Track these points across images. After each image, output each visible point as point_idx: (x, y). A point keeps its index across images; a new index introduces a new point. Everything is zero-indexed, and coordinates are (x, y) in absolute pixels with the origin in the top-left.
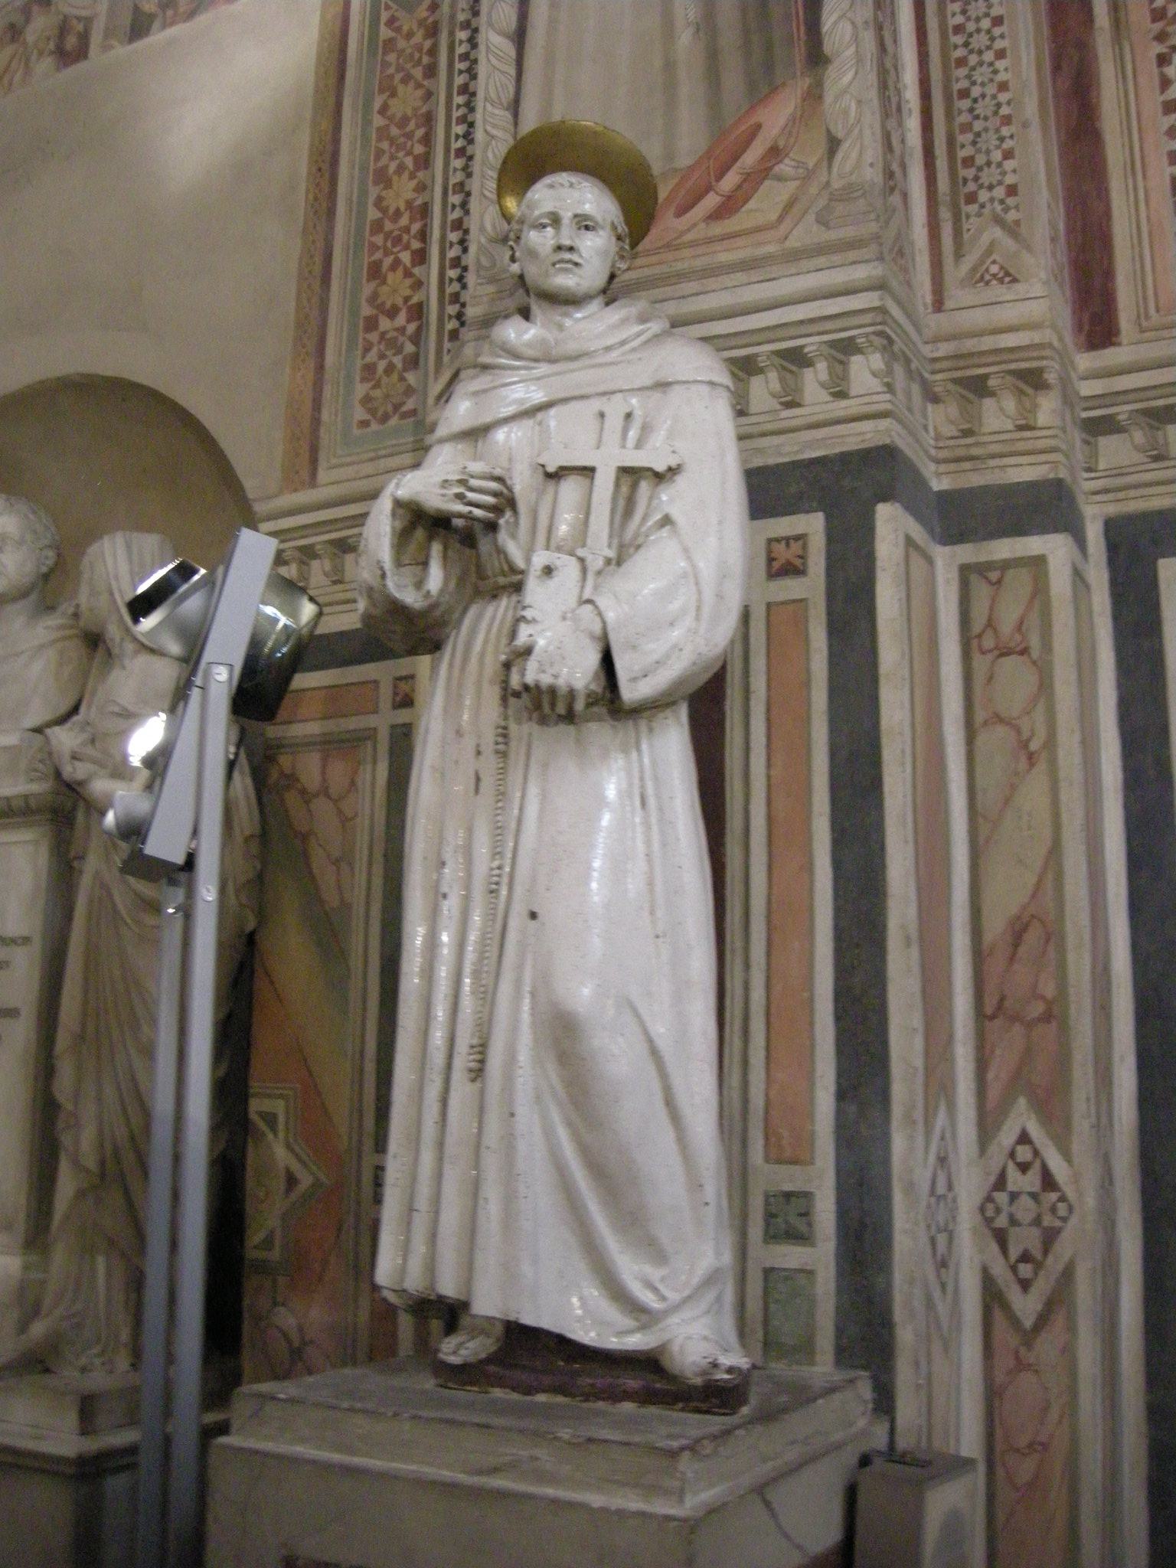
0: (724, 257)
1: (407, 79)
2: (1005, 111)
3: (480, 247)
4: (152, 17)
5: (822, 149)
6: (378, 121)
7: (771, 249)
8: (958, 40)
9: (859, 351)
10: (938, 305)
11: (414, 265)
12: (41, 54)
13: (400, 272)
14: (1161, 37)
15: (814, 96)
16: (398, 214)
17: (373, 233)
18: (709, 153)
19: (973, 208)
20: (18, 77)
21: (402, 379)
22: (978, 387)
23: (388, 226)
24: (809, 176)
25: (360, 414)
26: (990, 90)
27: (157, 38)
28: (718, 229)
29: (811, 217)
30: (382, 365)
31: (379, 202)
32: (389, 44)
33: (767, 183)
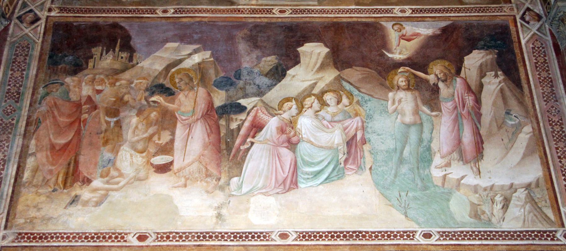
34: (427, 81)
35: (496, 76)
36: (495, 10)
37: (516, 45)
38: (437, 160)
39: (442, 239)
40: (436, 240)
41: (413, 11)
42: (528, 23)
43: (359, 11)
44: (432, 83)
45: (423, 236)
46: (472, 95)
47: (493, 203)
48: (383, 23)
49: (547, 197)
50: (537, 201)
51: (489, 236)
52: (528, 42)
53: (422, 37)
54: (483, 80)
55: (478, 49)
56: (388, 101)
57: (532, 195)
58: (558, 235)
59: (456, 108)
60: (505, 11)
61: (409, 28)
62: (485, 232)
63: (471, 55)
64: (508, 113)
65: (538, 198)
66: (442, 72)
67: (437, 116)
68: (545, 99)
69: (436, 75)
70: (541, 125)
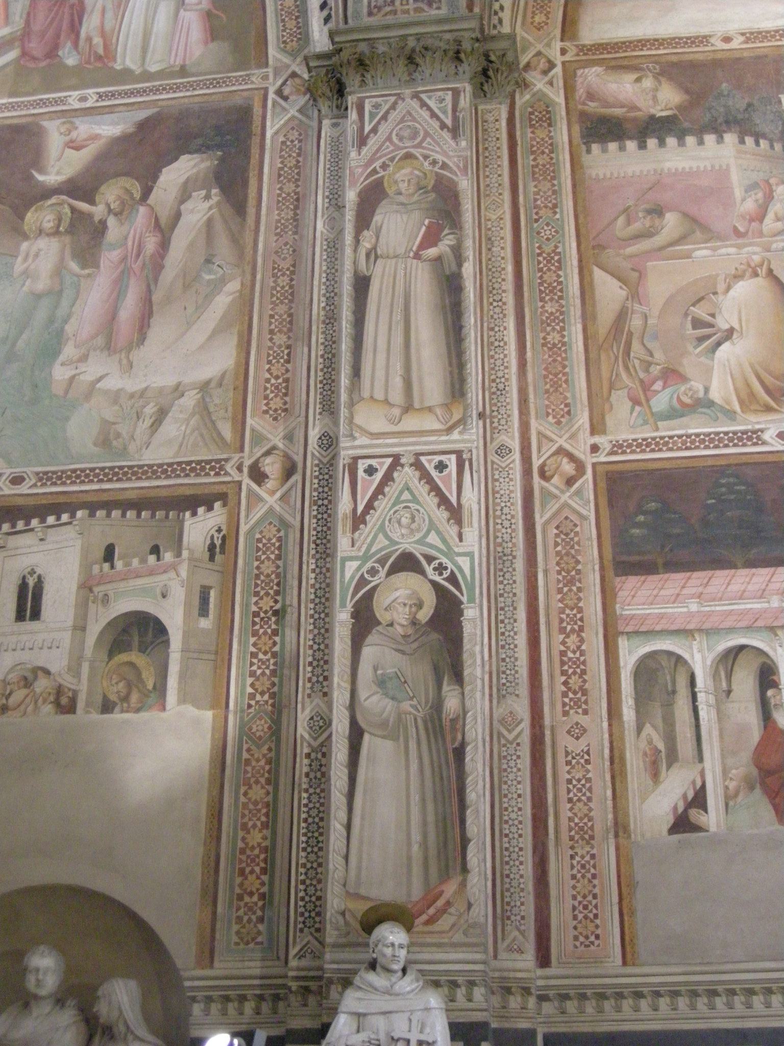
0: (429, 940)
1: (257, 782)
2: (522, 886)
3: (332, 914)
4: (114, 704)
5: (466, 906)
6: (242, 799)
7: (446, 940)
8: (507, 853)
9: (476, 985)
10: (495, 957)
11: (261, 874)
12: (45, 701)
13: (254, 876)
14: (572, 848)
15: (463, 884)
16: (253, 848)
17: (241, 853)
18: (423, 898)
19: (509, 922)
20: (30, 708)
21: (255, 926)
22: (508, 991)
23: (248, 852)
24: (460, 916)
25: (235, 939)
26: (517, 876)
27: (117, 716)
28: (427, 929)
29: (461, 931)
30: (246, 918)
31: (243, 839)
32: (248, 762)
33: (445, 915)
34: (90, 216)
35: (207, 197)
36: (237, 81)
37: (256, 140)
38: (69, 351)
39: (39, 484)
40: (31, 487)
41: (100, 97)
42: (286, 99)
43: (19, 105)
44: (97, 219)
45: (10, 482)
46: (159, 235)
47: (138, 418)
48: (45, 124)
49: (231, 402)
50: (212, 409)
51: (78, 477)
52: (276, 133)
53: (103, 141)
54: (182, 207)
55: (190, 153)
56: (16, 257)
57: (208, 400)
58: (228, 467)
59: (124, 259)
60: (253, 82)
61: (84, 128)
62: (112, 468)
63: (175, 165)
64: (208, 261)
65: (215, 405)
66: (119, 197)
67: (89, 275)
68: (279, 230)
69: (108, 205)
70: (259, 277)
